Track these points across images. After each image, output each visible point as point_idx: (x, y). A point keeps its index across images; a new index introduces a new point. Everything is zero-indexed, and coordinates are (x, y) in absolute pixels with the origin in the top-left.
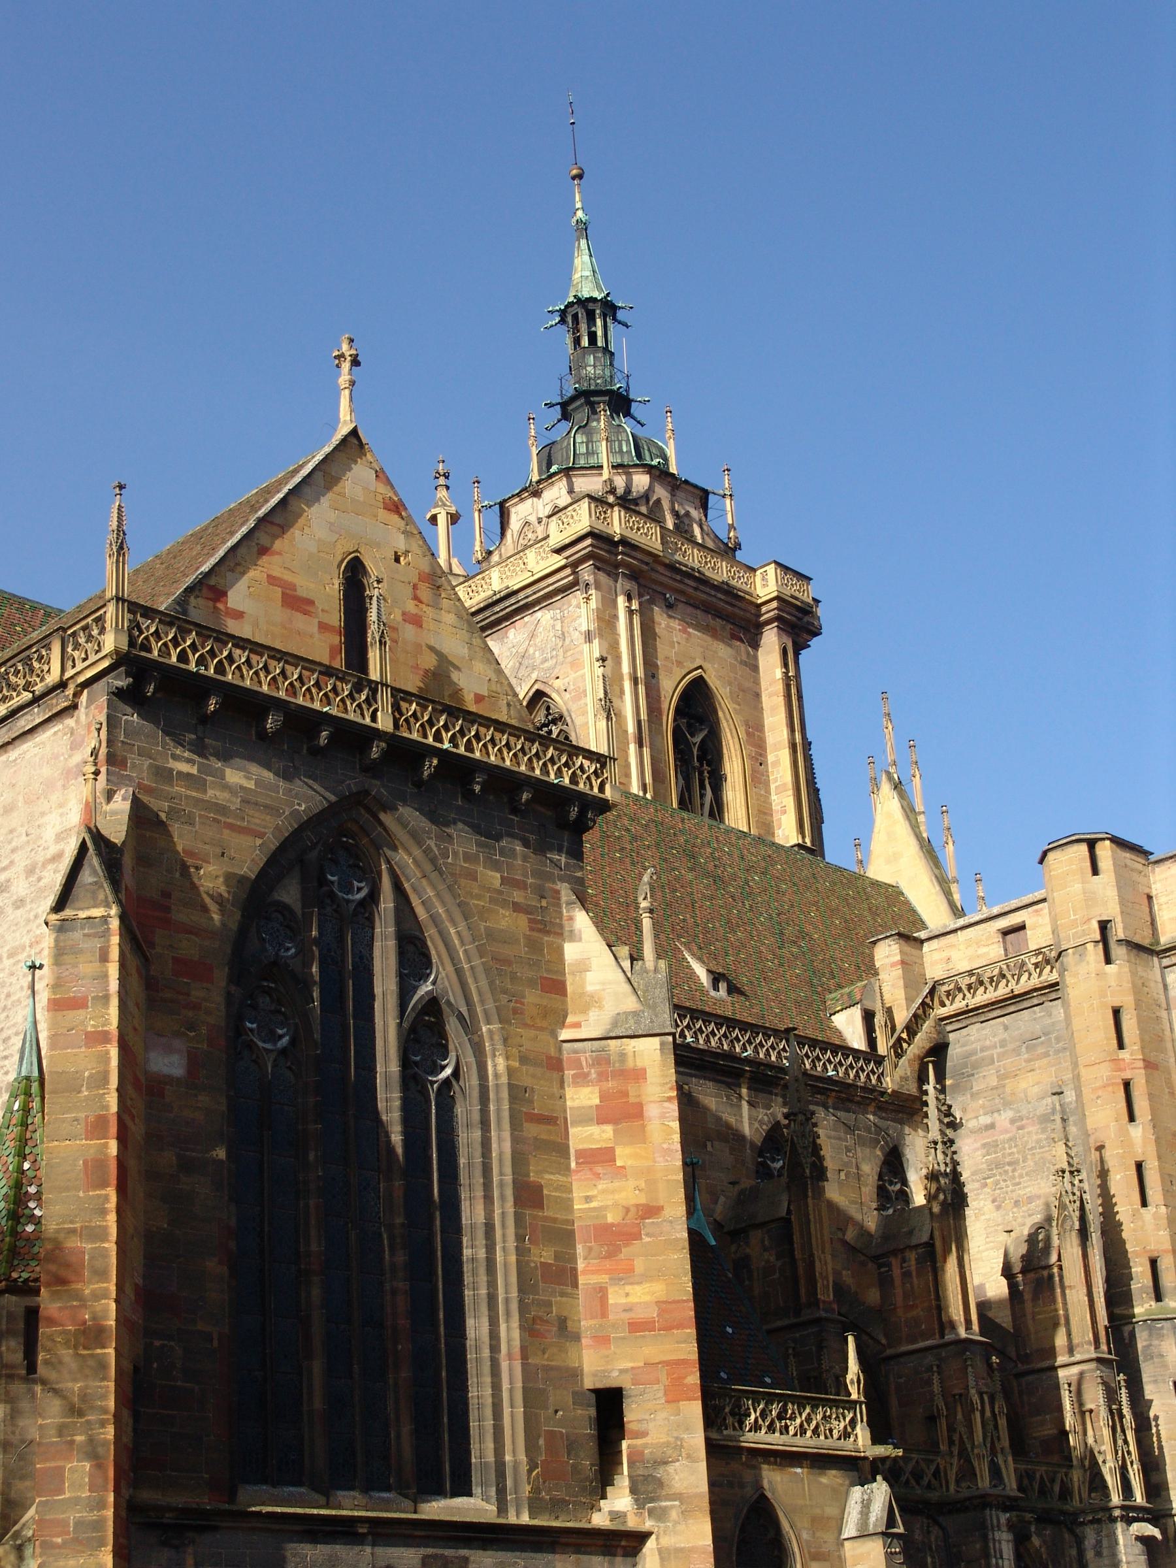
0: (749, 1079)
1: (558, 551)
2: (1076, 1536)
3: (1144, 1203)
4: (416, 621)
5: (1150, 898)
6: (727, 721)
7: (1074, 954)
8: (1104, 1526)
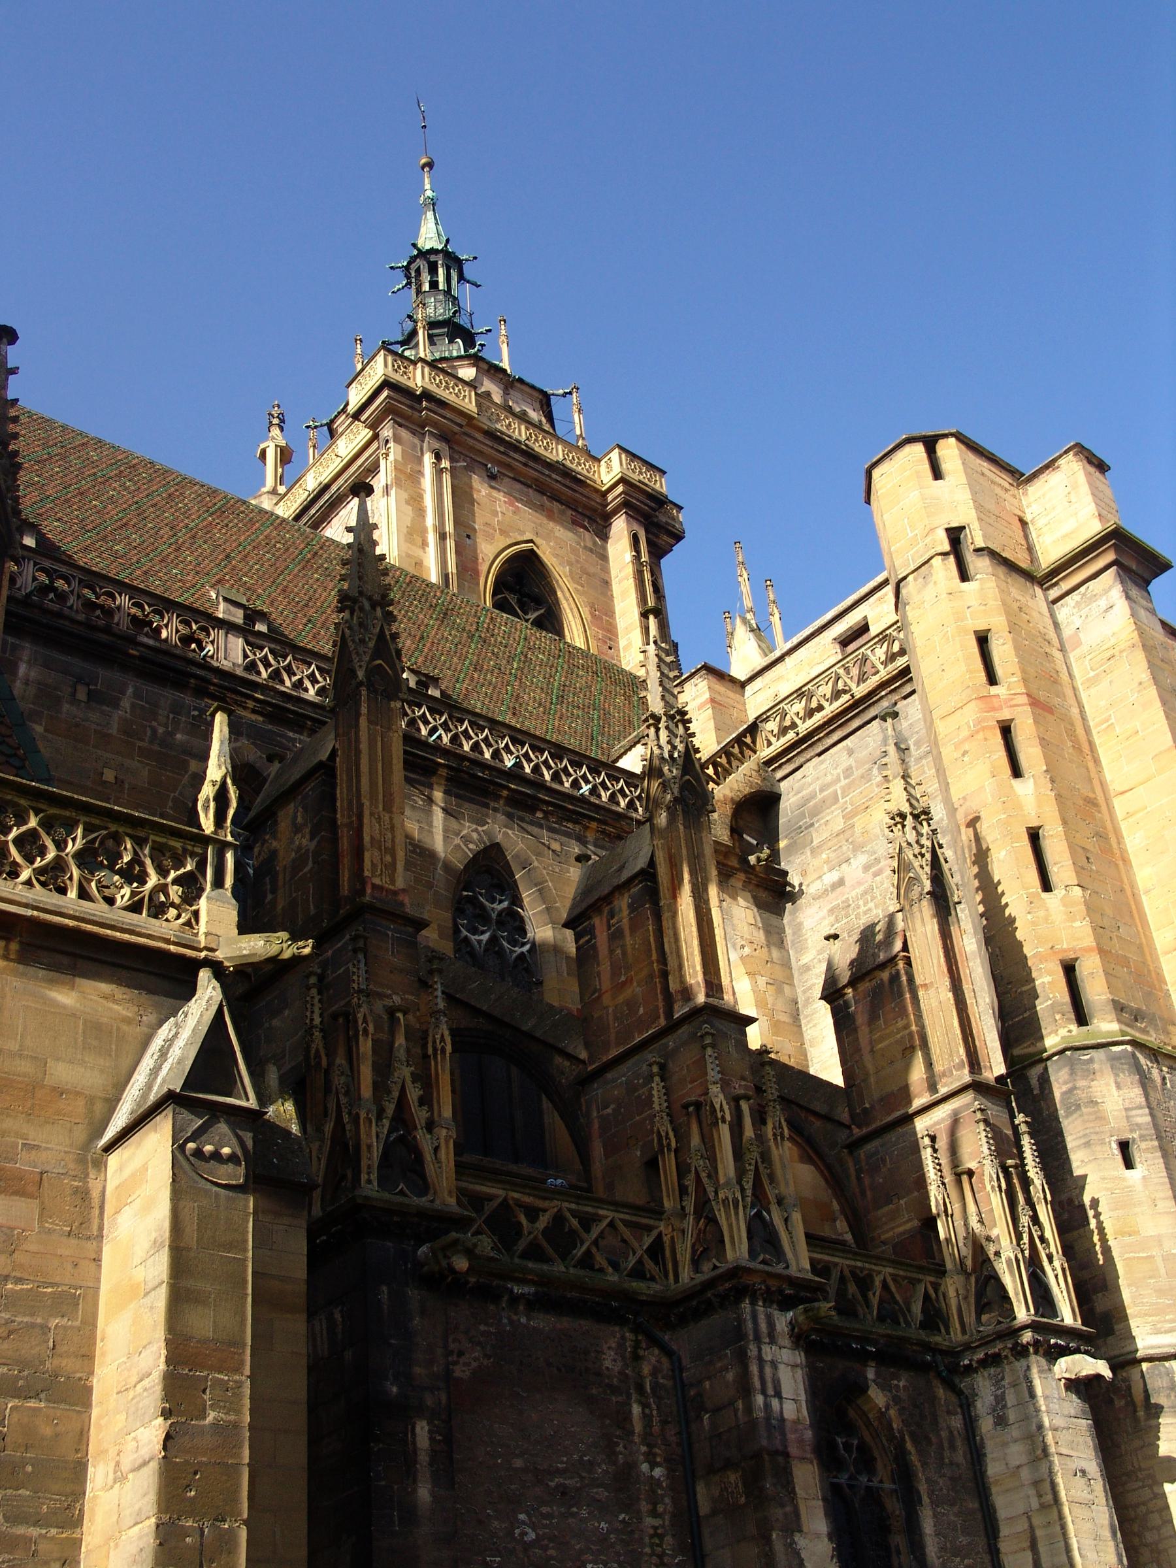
0: (448, 779)
2: (959, 1393)
3: (1047, 886)
5: (1023, 523)
6: (567, 600)
7: (915, 579)
8: (1007, 1368)
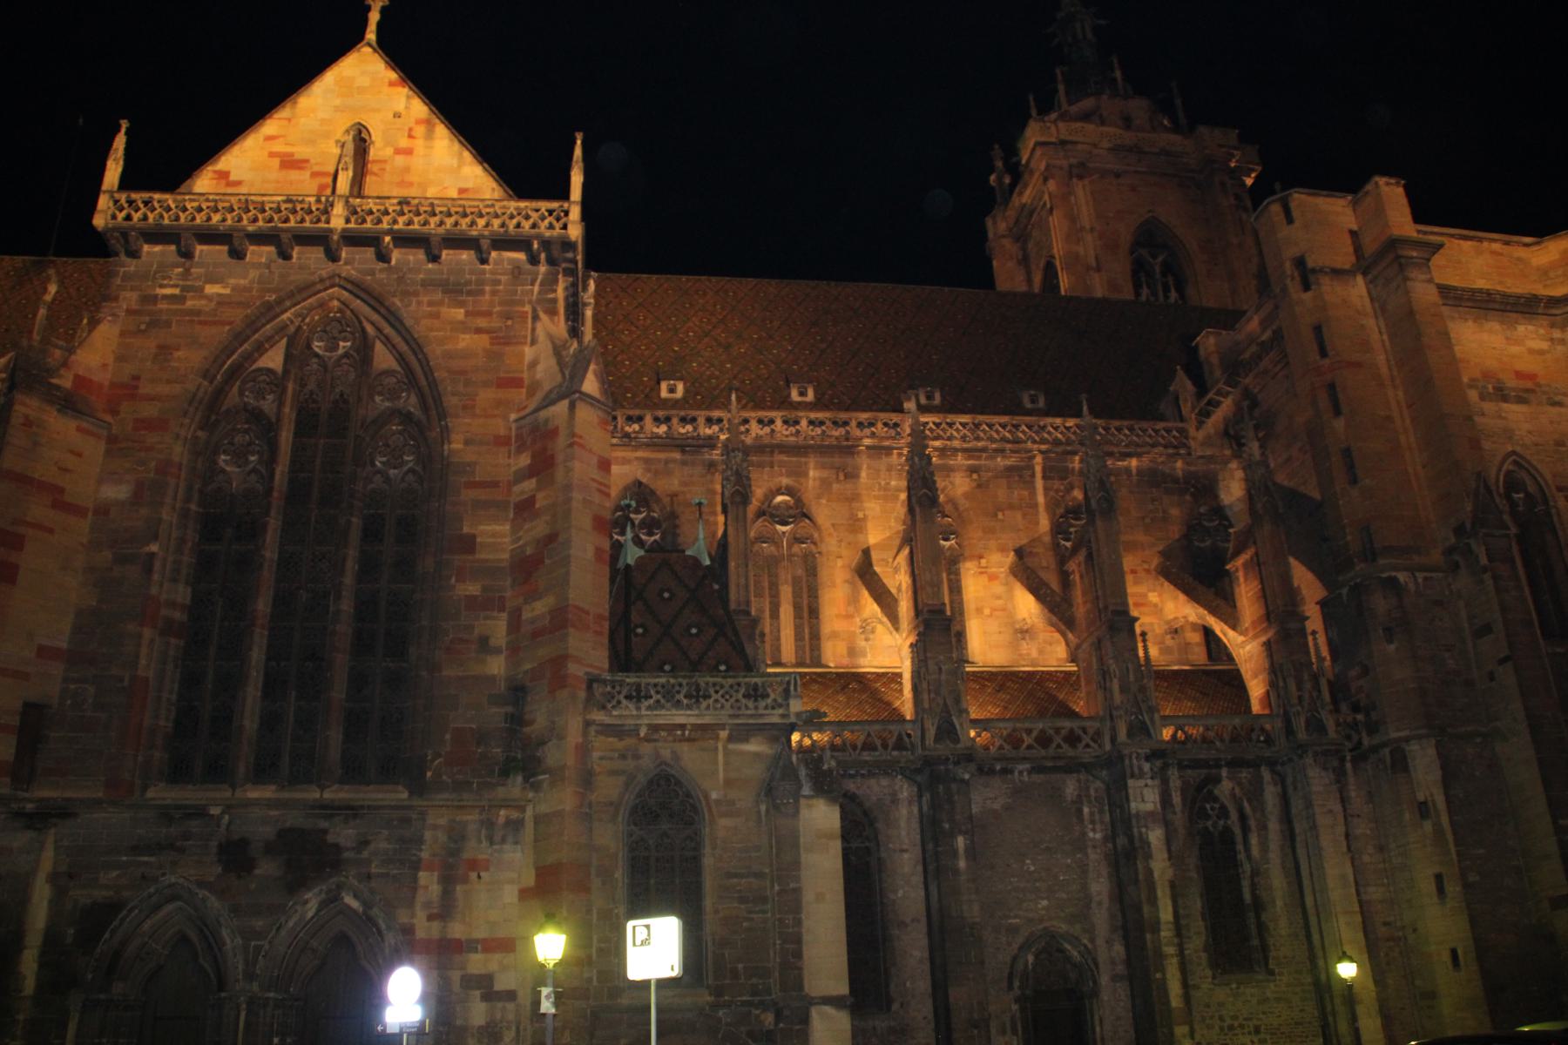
4: (408, 152)
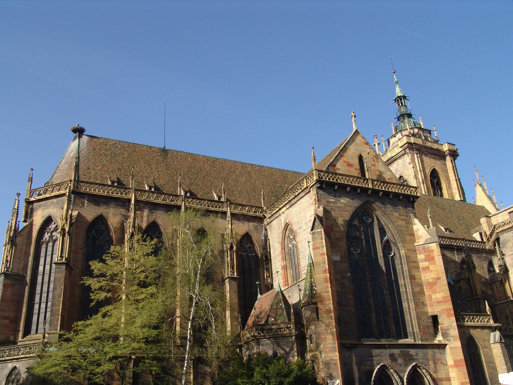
1: (401, 147)
4: (374, 165)
